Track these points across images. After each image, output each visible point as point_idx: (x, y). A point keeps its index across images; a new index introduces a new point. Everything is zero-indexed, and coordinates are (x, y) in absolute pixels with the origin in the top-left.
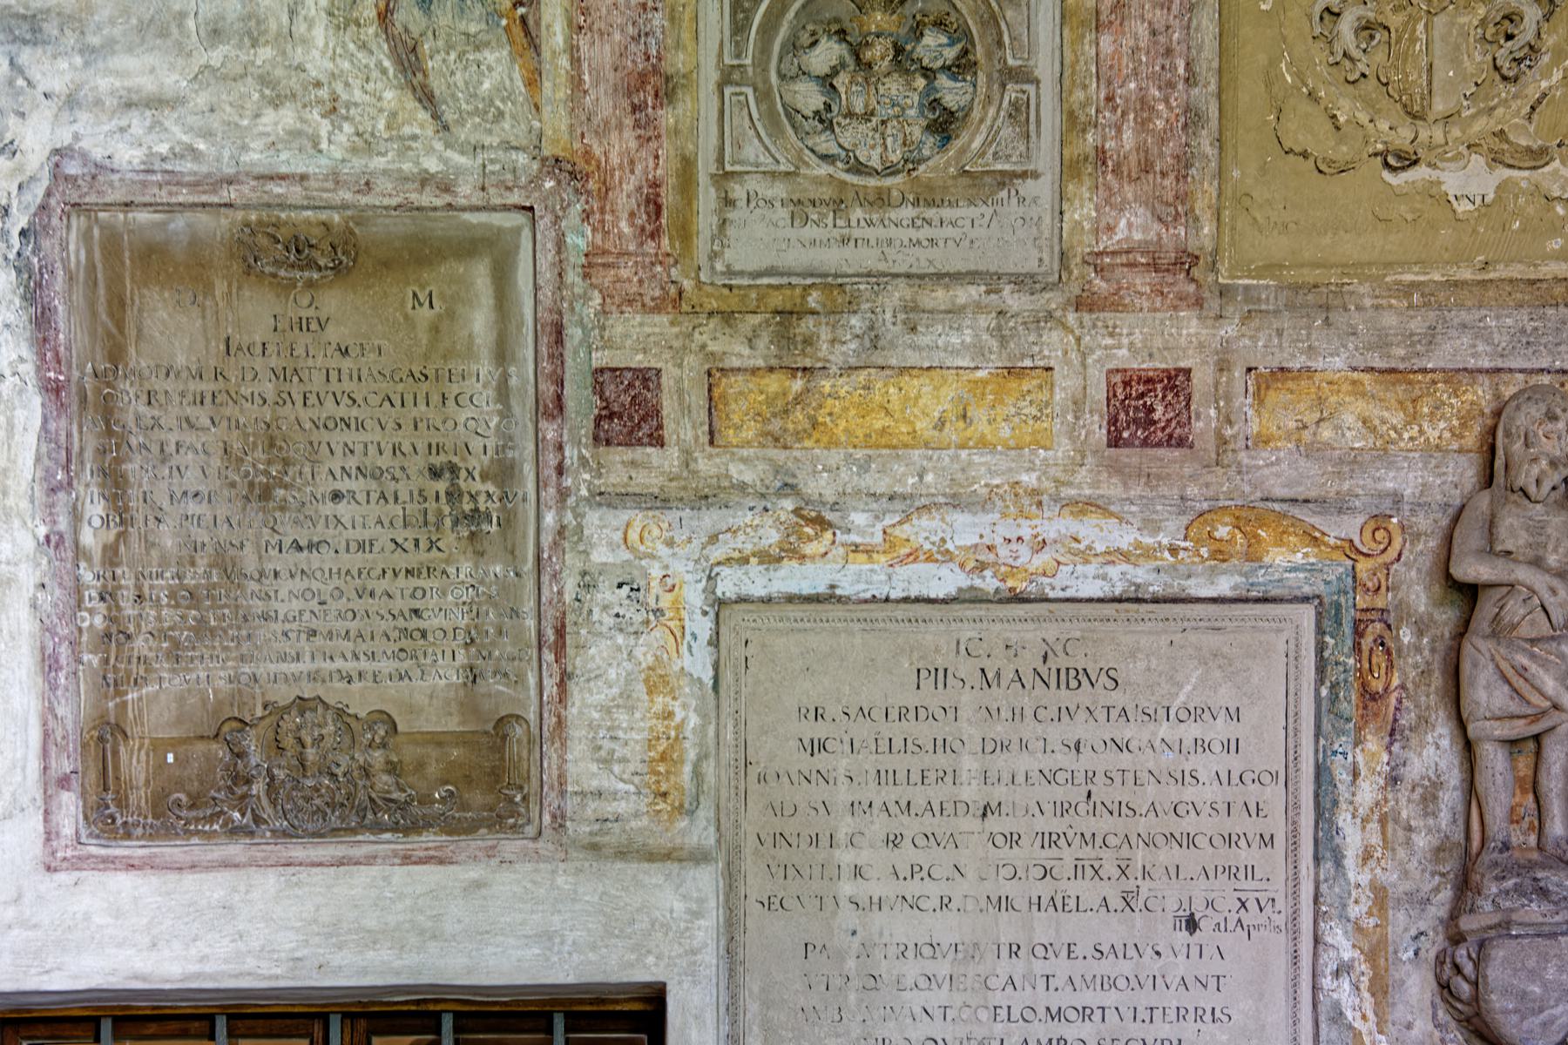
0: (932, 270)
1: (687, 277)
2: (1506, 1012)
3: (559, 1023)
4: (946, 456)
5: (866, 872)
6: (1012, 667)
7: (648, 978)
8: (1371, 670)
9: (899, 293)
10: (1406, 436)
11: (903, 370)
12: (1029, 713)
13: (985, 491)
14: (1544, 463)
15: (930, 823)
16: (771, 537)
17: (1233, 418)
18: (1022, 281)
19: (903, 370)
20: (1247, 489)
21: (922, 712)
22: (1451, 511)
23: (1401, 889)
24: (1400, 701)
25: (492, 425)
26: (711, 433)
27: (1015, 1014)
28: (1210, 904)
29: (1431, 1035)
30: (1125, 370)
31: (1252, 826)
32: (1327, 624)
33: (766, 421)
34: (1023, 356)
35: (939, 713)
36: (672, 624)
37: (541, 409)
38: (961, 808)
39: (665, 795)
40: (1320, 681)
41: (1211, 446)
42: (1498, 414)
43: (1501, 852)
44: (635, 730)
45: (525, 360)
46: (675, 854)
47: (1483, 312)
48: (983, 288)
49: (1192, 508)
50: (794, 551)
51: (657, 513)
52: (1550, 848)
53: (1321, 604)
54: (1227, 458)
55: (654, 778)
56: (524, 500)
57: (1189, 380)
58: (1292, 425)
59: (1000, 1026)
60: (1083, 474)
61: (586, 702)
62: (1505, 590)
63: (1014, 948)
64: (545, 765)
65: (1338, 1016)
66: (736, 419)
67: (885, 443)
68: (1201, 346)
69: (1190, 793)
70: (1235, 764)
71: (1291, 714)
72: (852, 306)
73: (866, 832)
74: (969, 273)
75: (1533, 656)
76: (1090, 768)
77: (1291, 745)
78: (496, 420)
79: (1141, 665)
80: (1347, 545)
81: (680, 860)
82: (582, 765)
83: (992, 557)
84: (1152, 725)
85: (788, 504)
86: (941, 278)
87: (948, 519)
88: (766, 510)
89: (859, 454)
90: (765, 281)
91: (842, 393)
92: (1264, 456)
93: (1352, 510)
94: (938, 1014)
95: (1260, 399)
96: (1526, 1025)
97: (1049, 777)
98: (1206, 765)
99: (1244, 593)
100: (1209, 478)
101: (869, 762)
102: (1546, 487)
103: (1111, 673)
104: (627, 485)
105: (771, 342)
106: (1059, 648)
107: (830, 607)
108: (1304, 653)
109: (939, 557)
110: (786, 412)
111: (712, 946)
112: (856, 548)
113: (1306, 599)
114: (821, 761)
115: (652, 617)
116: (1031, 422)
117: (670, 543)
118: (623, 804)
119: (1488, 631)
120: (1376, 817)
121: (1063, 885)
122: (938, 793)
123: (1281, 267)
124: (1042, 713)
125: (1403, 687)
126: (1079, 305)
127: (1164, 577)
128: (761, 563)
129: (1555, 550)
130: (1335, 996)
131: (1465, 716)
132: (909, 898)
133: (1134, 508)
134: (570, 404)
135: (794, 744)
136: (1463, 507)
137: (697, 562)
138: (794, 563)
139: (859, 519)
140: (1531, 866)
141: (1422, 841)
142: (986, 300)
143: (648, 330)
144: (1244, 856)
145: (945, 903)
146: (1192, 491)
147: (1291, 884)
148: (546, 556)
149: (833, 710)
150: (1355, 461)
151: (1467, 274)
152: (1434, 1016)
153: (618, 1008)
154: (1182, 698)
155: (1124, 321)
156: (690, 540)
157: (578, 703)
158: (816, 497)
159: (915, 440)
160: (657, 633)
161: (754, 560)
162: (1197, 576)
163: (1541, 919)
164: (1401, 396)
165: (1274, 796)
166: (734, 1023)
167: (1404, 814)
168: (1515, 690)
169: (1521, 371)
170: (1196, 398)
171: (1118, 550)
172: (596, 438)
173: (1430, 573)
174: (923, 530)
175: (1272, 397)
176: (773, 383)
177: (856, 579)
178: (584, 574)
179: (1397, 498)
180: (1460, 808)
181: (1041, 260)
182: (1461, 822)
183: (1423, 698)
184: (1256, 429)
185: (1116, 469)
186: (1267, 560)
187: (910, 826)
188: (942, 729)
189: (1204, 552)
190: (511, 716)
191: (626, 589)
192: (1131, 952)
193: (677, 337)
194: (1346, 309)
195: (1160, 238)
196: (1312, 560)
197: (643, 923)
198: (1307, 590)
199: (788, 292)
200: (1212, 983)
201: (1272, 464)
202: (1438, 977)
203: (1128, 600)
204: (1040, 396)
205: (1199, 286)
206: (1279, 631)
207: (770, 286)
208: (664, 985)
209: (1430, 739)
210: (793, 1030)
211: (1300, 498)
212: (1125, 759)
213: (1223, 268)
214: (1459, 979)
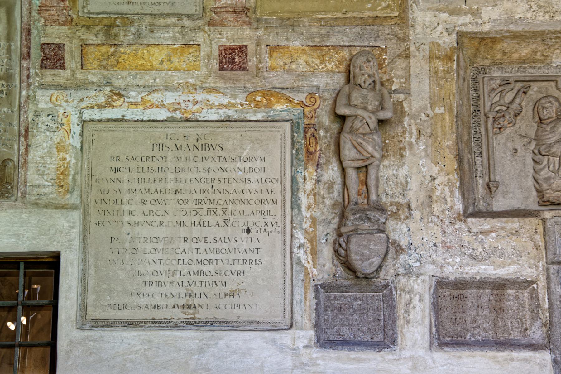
0: (159, 13)
1: (74, 14)
2: (357, 260)
3: (22, 266)
4: (163, 73)
5: (134, 213)
6: (186, 143)
7: (54, 249)
8: (310, 144)
9: (147, 20)
10: (320, 67)
11: (149, 45)
12: (192, 159)
13: (177, 85)
14: (366, 76)
15: (156, 196)
16: (102, 100)
17: (262, 61)
18: (189, 17)
19: (149, 45)
20: (267, 84)
21: (154, 158)
22: (336, 92)
23: (321, 218)
24: (320, 155)
25: (5, 62)
26: (82, 65)
27: (186, 262)
28: (255, 224)
29: (332, 269)
30: (225, 45)
31: (269, 197)
32: (295, 129)
33: (101, 61)
34: (190, 41)
35: (160, 159)
36: (66, 128)
37: (22, 56)
38: (168, 191)
39: (62, 186)
40: (293, 148)
41: (255, 71)
42: (351, 60)
43: (355, 205)
44: (52, 164)
45: (17, 40)
46: (65, 207)
47: (346, 27)
48: (176, 19)
49: (248, 91)
50: (110, 104)
51: (62, 91)
52: (371, 203)
53: (293, 122)
54: (260, 75)
55: (59, 181)
56: (15, 87)
57: (247, 49)
58: (282, 63)
59: (180, 266)
60: (210, 80)
61: (35, 155)
62: (354, 117)
63: (186, 239)
64: (20, 176)
65: (299, 262)
66: (91, 61)
67: (142, 68)
68: (251, 38)
69: (248, 186)
70: (264, 176)
71: (283, 159)
72: (131, 24)
73: (134, 199)
74: (171, 14)
75: (364, 139)
76: (213, 177)
77: (283, 170)
78: (6, 60)
79: (231, 143)
80: (301, 103)
81: (67, 209)
82: (33, 176)
83: (179, 107)
84: (235, 163)
85: (108, 89)
86: (161, 15)
87: (164, 94)
88: (101, 91)
89: (133, 72)
90: (101, 16)
91: (128, 52)
92: (271, 74)
93: (303, 91)
94: (158, 262)
95: (271, 55)
96: (363, 265)
97: (199, 181)
98: (253, 176)
99: (266, 119)
100: (254, 81)
101: (135, 175)
102: (367, 83)
103: (221, 145)
104: (51, 82)
105: (103, 36)
106: (202, 137)
107: (122, 123)
108: (287, 139)
109: (161, 106)
110: (108, 58)
111: (77, 239)
112: (132, 103)
113: (287, 121)
114: (118, 175)
115: (59, 126)
116: (193, 62)
117: (67, 101)
118: (47, 189)
119: (349, 131)
120: (312, 194)
121: (203, 217)
122: (159, 186)
123: (278, 12)
124: (196, 159)
125: (321, 150)
126: (209, 24)
127: (239, 113)
128: (98, 108)
129: (371, 104)
130: (298, 255)
131: (342, 159)
132: (148, 222)
133: (228, 91)
134: (33, 55)
135: (108, 169)
136: (340, 91)
137: (76, 108)
138: (110, 108)
139: (133, 94)
140: (365, 210)
141: (328, 202)
142: (177, 22)
143: (60, 31)
144: (266, 207)
145: (161, 224)
146: (248, 85)
147: (283, 217)
148: (22, 105)
149: (123, 158)
150: (303, 75)
151: (340, 15)
152: (333, 262)
153: (44, 260)
154: (245, 154)
155: (224, 30)
156: (73, 101)
157: (32, 155)
158: (118, 86)
159: (152, 68)
160: (61, 131)
161: (96, 107)
162: (250, 113)
163: (368, 228)
164: (319, 54)
165: (277, 187)
166: (84, 265)
167: (322, 193)
168: (358, 151)
169: (359, 46)
170: (249, 55)
171: (223, 104)
172: (41, 67)
173: (329, 112)
174: (155, 97)
175: (275, 54)
176: (104, 49)
177: (131, 114)
178: (36, 111)
179: (318, 87)
180: (341, 190)
181: (196, 10)
182: (341, 195)
183: (328, 154)
184: (269, 65)
185: (222, 78)
186: (274, 108)
187: (149, 197)
188: (161, 164)
189: (252, 105)
190: (8, 159)
191: (51, 116)
192: (227, 240)
193: (71, 33)
194: (299, 26)
195: (236, 3)
196: (289, 108)
197: (53, 231)
198: (288, 118)
199: (109, 19)
200: (255, 251)
201: (275, 76)
202: (334, 248)
203: (226, 121)
204: (196, 54)
205: (250, 18)
206: (279, 131)
207: (103, 17)
208: (60, 252)
209: (330, 167)
210: (106, 267)
211: (285, 87)
212: (225, 175)
213: (258, 12)
214: (341, 249)
